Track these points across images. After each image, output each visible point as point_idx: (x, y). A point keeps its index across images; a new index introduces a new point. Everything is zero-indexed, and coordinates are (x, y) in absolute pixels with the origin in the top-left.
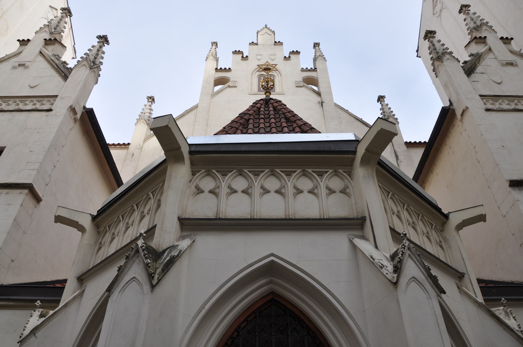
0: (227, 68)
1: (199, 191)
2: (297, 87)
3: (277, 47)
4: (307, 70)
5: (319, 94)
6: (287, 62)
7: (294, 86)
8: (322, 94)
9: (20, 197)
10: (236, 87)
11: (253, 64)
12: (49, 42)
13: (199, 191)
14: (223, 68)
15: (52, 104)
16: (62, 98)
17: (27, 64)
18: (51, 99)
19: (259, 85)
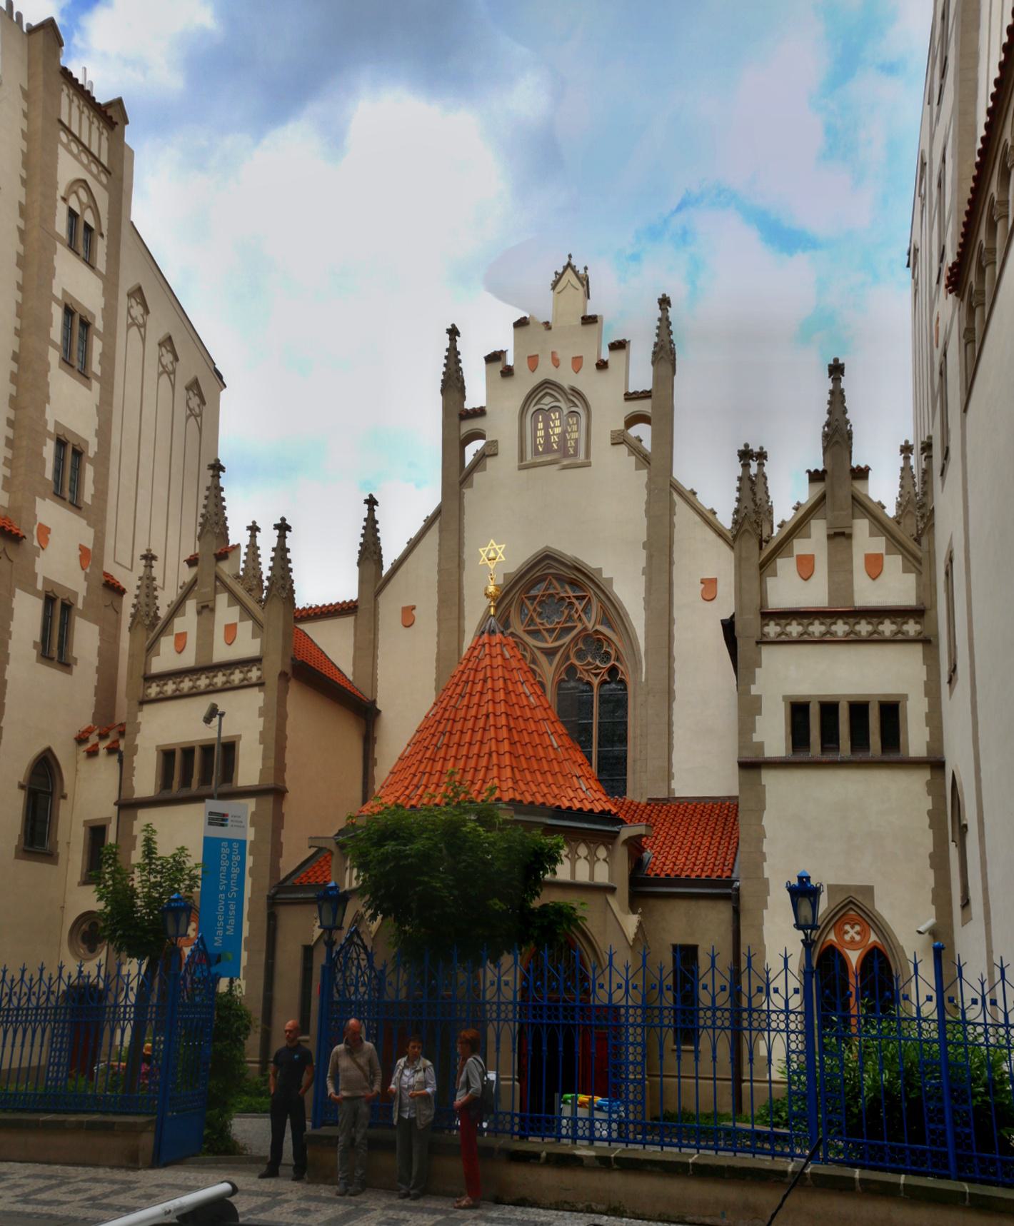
7: (609, 441)
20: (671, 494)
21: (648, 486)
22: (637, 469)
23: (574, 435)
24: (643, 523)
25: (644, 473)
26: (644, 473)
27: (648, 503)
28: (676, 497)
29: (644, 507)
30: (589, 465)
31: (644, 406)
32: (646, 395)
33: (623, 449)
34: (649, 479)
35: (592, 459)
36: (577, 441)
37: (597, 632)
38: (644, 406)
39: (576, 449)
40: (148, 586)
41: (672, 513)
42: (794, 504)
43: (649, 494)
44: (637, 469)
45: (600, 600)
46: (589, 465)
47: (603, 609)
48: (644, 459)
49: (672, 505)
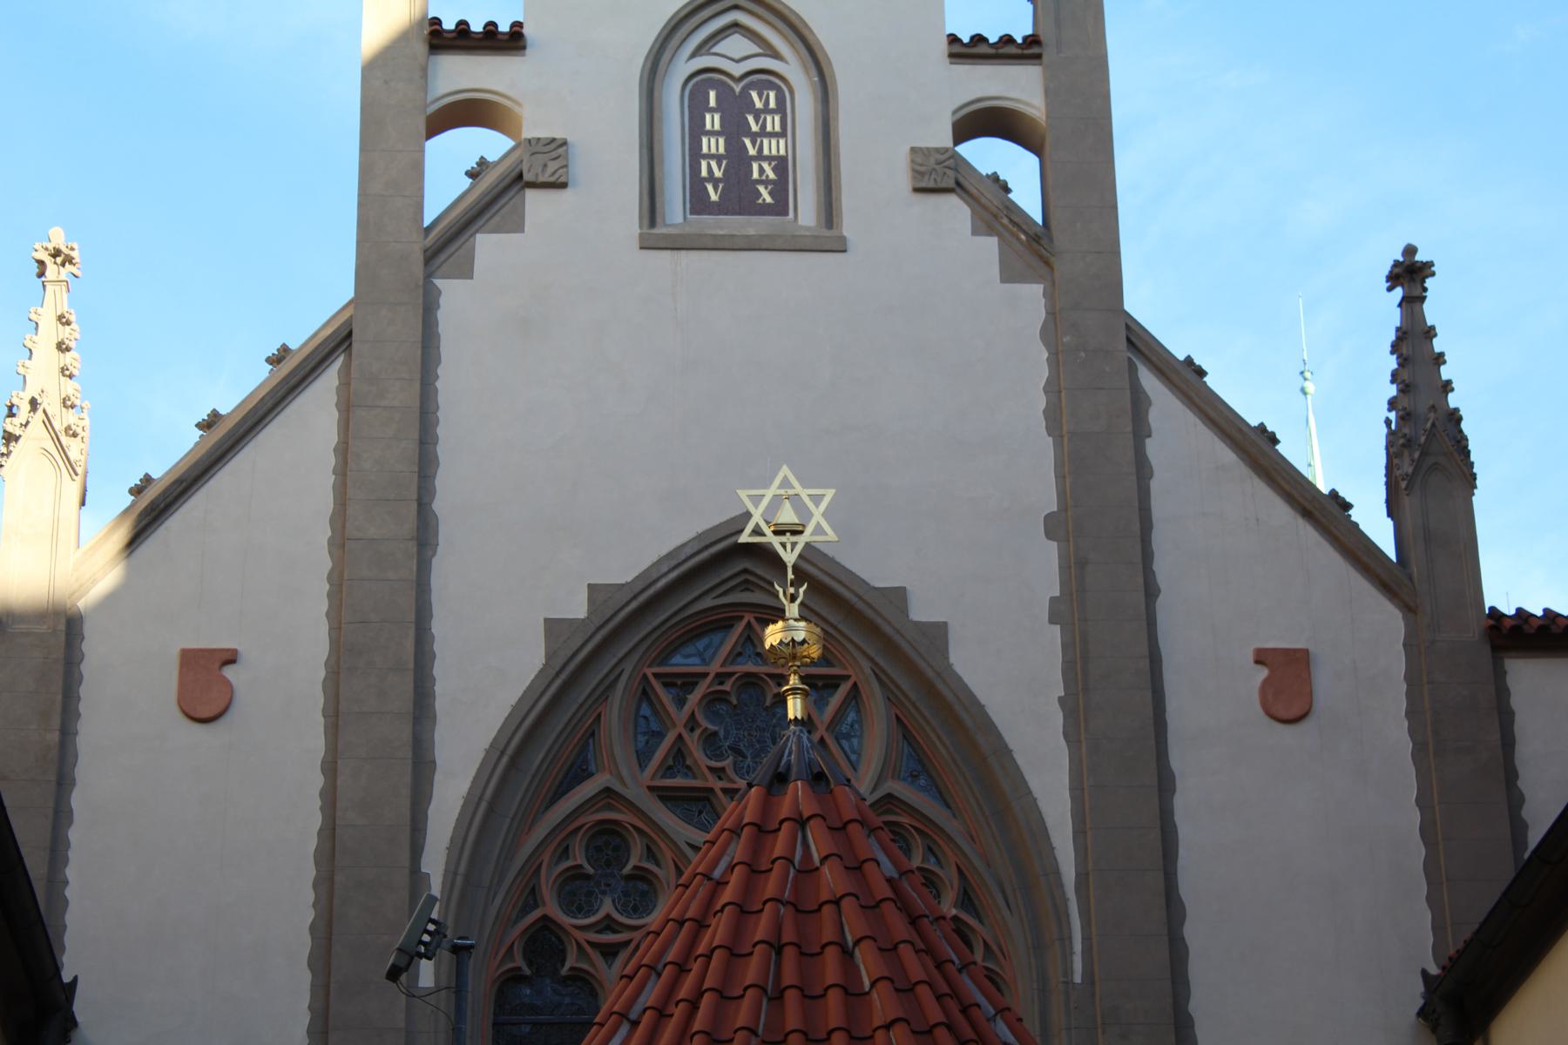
0: (504, 27)
2: (917, 190)
10: (564, 185)
14: (477, 27)
19: (695, 155)
20: (1132, 370)
21: (1050, 333)
22: (1008, 276)
23: (772, 147)
24: (1041, 453)
25: (1032, 295)
26: (1032, 295)
27: (1053, 389)
28: (1149, 381)
29: (1042, 402)
30: (840, 247)
31: (1020, 87)
32: (1005, 51)
33: (955, 210)
34: (1052, 314)
35: (849, 226)
36: (781, 164)
37: (889, 802)
38: (1020, 87)
39: (781, 188)
41: (1141, 431)
43: (1054, 362)
44: (1008, 276)
45: (893, 697)
46: (840, 247)
47: (903, 728)
48: (1030, 248)
49: (1139, 402)
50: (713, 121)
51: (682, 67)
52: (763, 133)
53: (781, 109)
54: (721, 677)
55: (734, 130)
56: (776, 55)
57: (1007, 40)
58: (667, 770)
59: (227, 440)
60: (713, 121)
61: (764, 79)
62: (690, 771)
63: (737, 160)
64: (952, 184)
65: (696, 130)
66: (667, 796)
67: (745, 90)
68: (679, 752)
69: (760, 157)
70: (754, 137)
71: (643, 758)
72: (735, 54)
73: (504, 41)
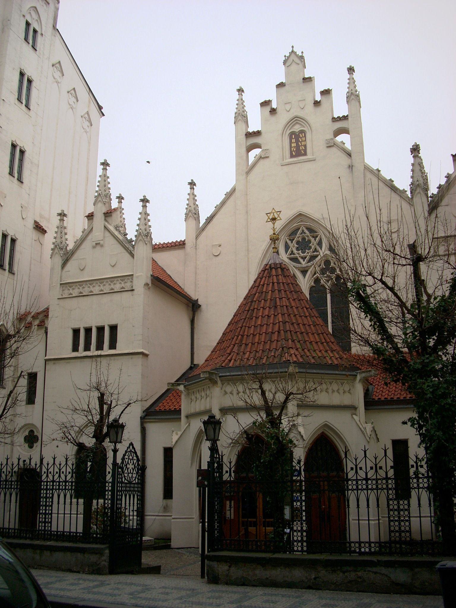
1: (226, 393)
2: (327, 147)
3: (308, 85)
4: (339, 119)
5: (349, 155)
6: (318, 109)
7: (325, 145)
8: (352, 155)
9: (139, 360)
10: (268, 157)
11: (283, 118)
12: (107, 215)
13: (226, 393)
15: (131, 282)
16: (137, 277)
17: (102, 242)
18: (130, 278)
19: (291, 147)
23: (303, 143)
33: (334, 150)
36: (305, 146)
39: (305, 151)
40: (61, 229)
42: (446, 175)
50: (293, 141)
51: (288, 132)
52: (302, 141)
53: (305, 136)
54: (298, 237)
55: (297, 141)
56: (304, 127)
57: (344, 116)
58: (291, 254)
59: (219, 208)
60: (293, 141)
61: (302, 132)
62: (294, 254)
63: (298, 147)
64: (332, 144)
65: (291, 143)
66: (291, 259)
67: (299, 134)
68: (292, 252)
69: (302, 146)
70: (301, 142)
71: (286, 252)
72: (297, 128)
73: (258, 133)
